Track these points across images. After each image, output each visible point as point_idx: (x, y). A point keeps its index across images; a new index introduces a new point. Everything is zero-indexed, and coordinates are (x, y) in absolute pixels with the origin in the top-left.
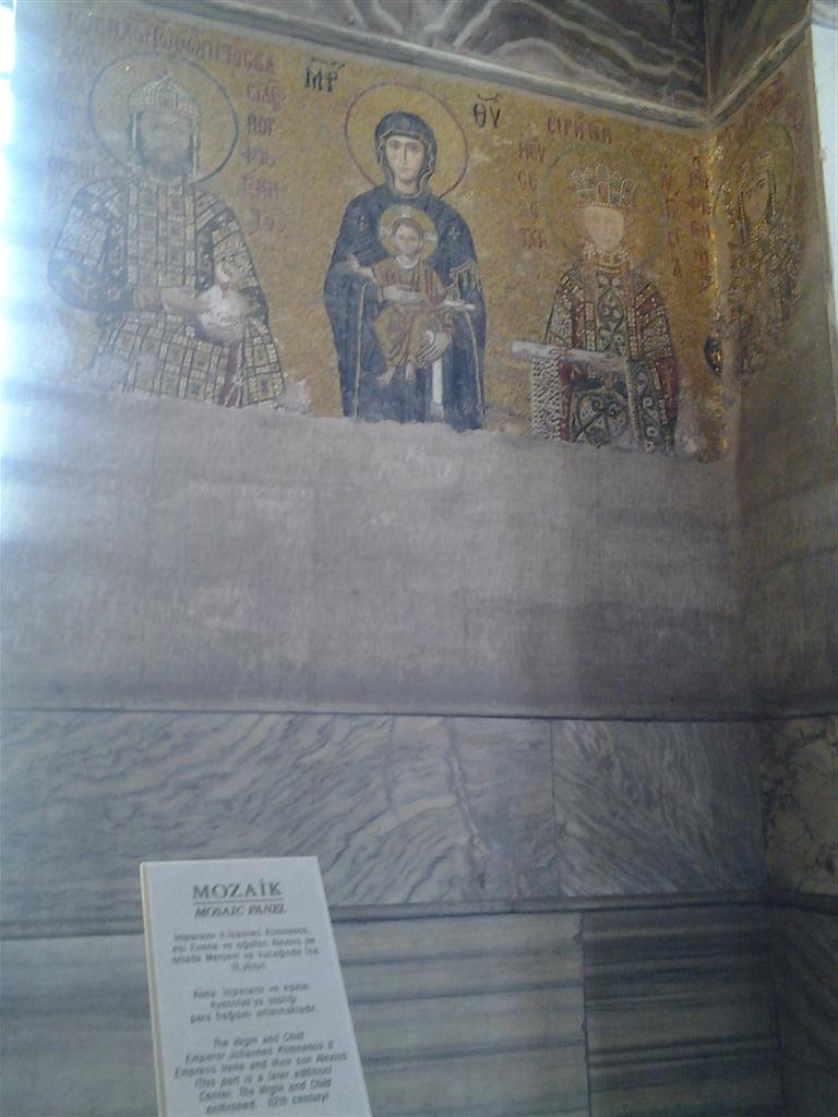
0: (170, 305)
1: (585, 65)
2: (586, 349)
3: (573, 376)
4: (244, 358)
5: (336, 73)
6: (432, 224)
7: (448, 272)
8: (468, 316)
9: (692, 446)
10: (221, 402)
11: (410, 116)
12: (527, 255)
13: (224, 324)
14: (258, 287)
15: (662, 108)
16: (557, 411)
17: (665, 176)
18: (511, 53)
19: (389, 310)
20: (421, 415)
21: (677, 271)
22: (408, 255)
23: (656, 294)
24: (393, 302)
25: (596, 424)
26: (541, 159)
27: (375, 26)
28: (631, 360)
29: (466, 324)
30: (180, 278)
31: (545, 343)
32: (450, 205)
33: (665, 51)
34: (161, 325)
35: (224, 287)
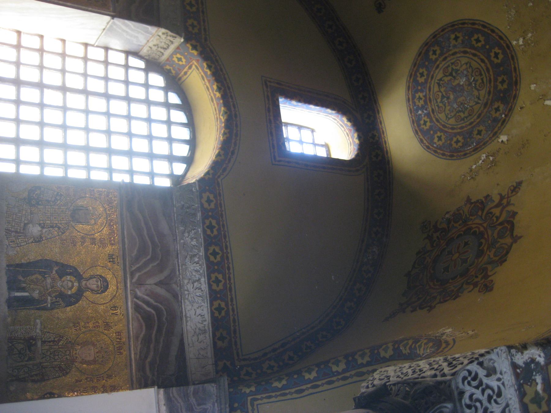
0: (33, 216)
1: (141, 343)
2: (42, 346)
3: (31, 341)
4: (20, 236)
5: (115, 263)
6: (74, 292)
7: (59, 298)
8: (45, 304)
9: (12, 388)
10: (6, 229)
11: (108, 285)
12: (71, 325)
13: (30, 231)
14: (43, 240)
15: (134, 371)
16: (18, 335)
17: (111, 376)
18: (138, 318)
19: (43, 279)
20: (10, 289)
21: (77, 381)
22: (62, 285)
23: (67, 373)
24: (45, 280)
25: (15, 350)
26: (104, 330)
27: (132, 274)
28: (41, 363)
29: (44, 304)
30: (42, 219)
31: (41, 331)
32: (81, 298)
33: (156, 373)
34: (27, 214)
35: (41, 231)
